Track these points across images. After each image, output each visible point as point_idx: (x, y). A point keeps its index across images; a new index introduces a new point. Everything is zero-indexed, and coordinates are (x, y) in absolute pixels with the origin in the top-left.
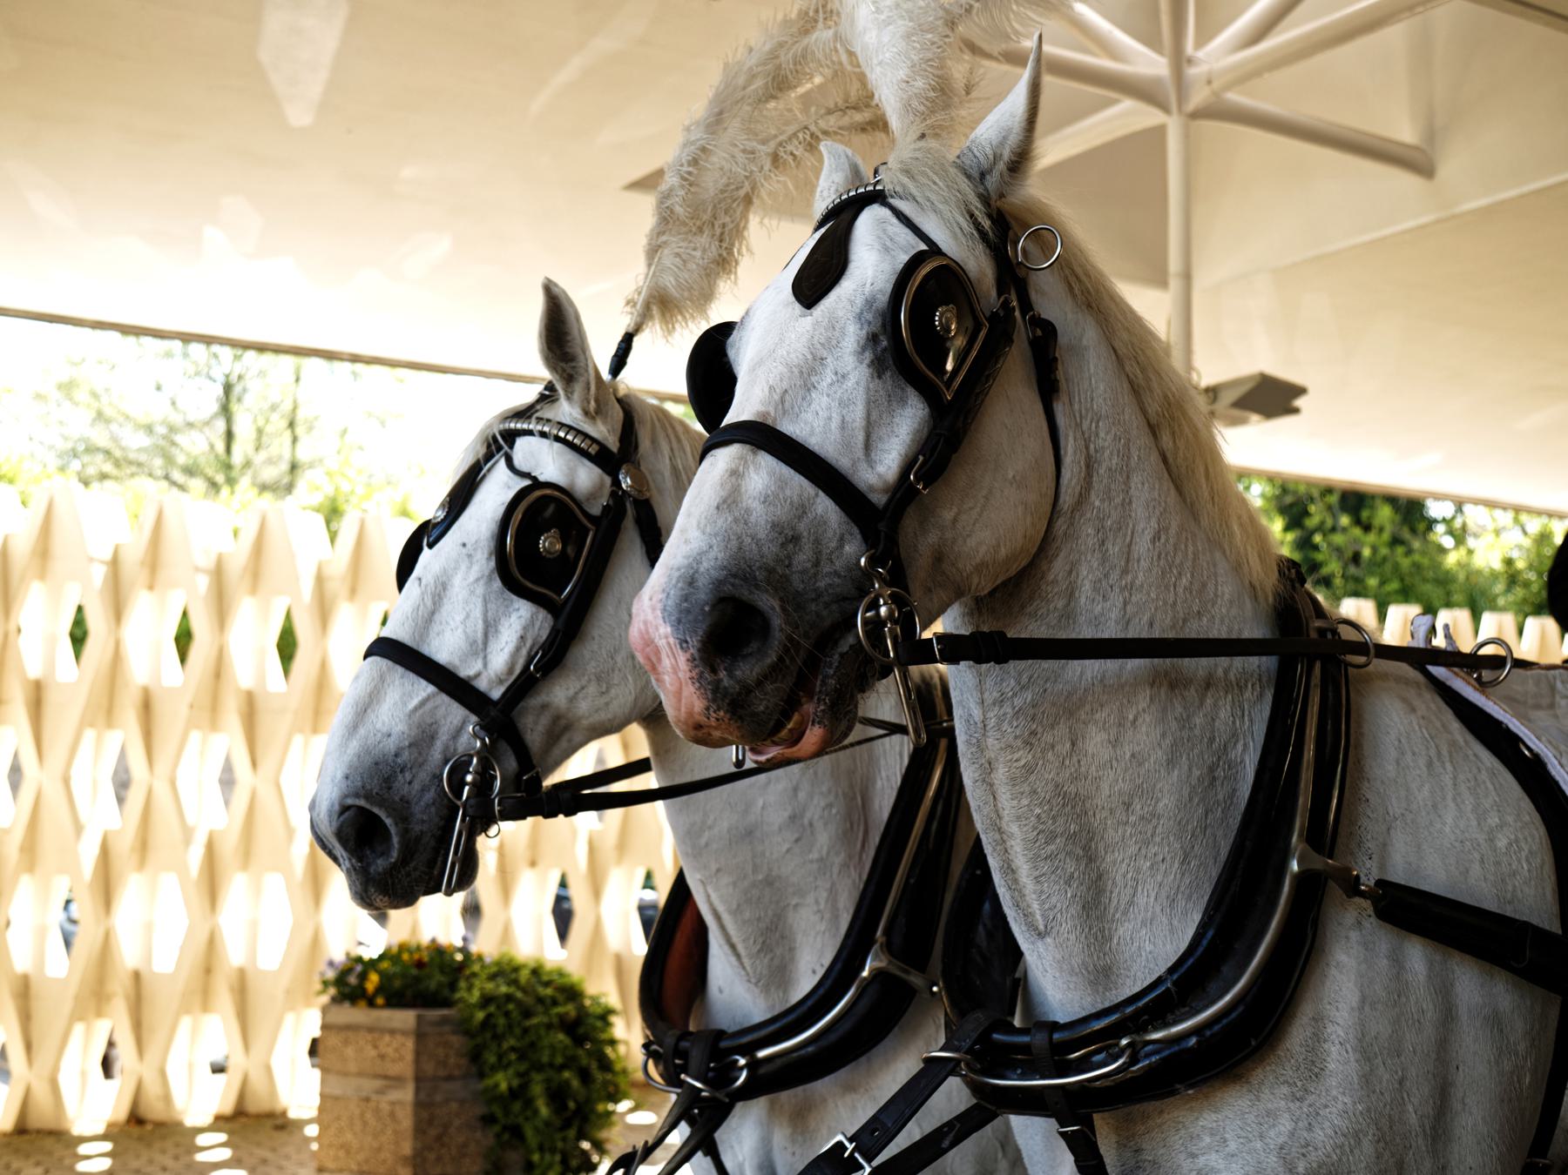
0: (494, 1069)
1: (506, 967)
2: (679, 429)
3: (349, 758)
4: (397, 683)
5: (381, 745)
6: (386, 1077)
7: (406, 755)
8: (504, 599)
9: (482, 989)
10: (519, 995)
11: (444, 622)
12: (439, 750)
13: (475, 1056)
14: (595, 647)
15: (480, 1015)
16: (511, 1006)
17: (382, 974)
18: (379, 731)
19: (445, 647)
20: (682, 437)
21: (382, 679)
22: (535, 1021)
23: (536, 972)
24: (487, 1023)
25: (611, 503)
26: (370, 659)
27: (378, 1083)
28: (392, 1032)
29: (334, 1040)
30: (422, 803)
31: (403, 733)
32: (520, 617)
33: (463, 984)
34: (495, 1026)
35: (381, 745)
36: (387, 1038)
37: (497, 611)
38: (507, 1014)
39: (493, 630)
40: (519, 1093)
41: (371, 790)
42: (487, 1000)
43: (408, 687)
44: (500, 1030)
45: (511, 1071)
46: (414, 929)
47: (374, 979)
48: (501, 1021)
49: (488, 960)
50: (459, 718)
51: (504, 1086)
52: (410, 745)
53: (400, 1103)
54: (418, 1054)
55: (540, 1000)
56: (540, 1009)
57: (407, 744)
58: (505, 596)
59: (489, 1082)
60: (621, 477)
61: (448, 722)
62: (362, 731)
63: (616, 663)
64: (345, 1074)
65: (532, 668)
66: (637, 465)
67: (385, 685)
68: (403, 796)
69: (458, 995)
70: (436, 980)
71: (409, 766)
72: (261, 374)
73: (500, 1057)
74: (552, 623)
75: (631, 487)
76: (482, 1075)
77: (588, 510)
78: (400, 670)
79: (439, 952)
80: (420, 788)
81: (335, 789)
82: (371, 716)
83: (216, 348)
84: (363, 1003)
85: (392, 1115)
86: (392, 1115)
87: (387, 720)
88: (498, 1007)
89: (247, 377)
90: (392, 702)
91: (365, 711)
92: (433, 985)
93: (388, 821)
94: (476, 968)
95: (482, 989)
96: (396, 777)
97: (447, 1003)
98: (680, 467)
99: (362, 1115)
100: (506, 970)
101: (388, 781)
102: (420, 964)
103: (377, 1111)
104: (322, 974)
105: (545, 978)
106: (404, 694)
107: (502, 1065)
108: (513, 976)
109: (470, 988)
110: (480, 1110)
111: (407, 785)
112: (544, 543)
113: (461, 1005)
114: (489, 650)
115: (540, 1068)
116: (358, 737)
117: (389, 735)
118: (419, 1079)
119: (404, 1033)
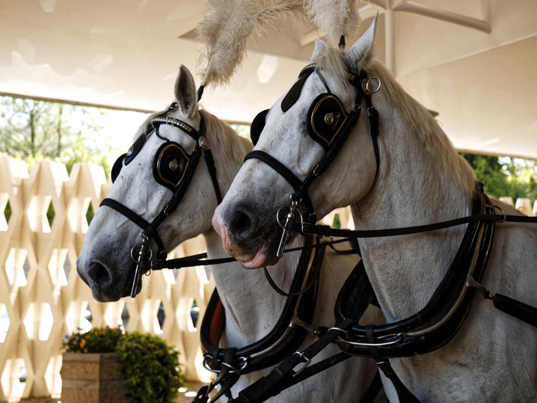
0: (131, 376)
1: (136, 336)
2: (221, 124)
3: (94, 244)
4: (113, 216)
5: (106, 240)
6: (88, 380)
7: (116, 245)
8: (155, 186)
9: (126, 345)
10: (141, 347)
11: (132, 194)
12: (128, 243)
13: (124, 371)
14: (189, 205)
15: (125, 355)
16: (137, 352)
17: (87, 340)
18: (106, 234)
19: (132, 203)
20: (221, 126)
21: (107, 214)
22: (147, 357)
23: (148, 338)
24: (128, 358)
25: (196, 150)
26: (102, 207)
27: (85, 383)
28: (91, 362)
29: (68, 366)
30: (122, 263)
31: (115, 236)
32: (161, 192)
33: (119, 343)
34: (131, 359)
35: (106, 240)
36: (89, 365)
37: (152, 190)
38: (136, 354)
39: (151, 197)
40: (140, 385)
41: (103, 257)
42: (128, 349)
43: (117, 218)
44: (133, 360)
45: (137, 376)
46: (103, 322)
47: (83, 342)
48: (134, 357)
49: (129, 334)
50: (136, 230)
51: (134, 382)
52: (118, 241)
53: (94, 390)
54: (101, 371)
55: (149, 349)
56: (149, 352)
57: (116, 240)
58: (155, 184)
59: (129, 381)
60: (199, 141)
61: (132, 232)
62: (99, 234)
63: (196, 211)
64: (72, 379)
65: (164, 211)
66: (205, 136)
67: (109, 217)
68: (115, 260)
69: (117, 348)
70: (108, 341)
71: (117, 249)
72: (46, 111)
73: (133, 371)
74: (172, 195)
75: (203, 145)
76: (126, 378)
77: (187, 152)
78: (114, 211)
79: (109, 330)
80: (121, 258)
81: (88, 256)
82: (103, 229)
83: (27, 101)
84: (79, 352)
85: (91, 395)
86: (91, 395)
87: (109, 231)
88: (132, 352)
89: (40, 112)
90: (111, 223)
91: (101, 226)
92: (107, 344)
93: (108, 270)
94: (124, 337)
95: (126, 345)
96: (112, 253)
97: (112, 351)
98: (220, 138)
99: (78, 395)
100: (136, 337)
101: (109, 254)
102: (102, 336)
103: (84, 393)
104: (63, 341)
105: (151, 340)
106: (116, 221)
107: (134, 374)
108: (139, 340)
109: (121, 345)
110: (126, 392)
111: (116, 256)
112: (171, 165)
113: (118, 352)
114: (149, 205)
115: (148, 374)
116: (97, 236)
117: (110, 236)
118: (101, 380)
119: (95, 363)
